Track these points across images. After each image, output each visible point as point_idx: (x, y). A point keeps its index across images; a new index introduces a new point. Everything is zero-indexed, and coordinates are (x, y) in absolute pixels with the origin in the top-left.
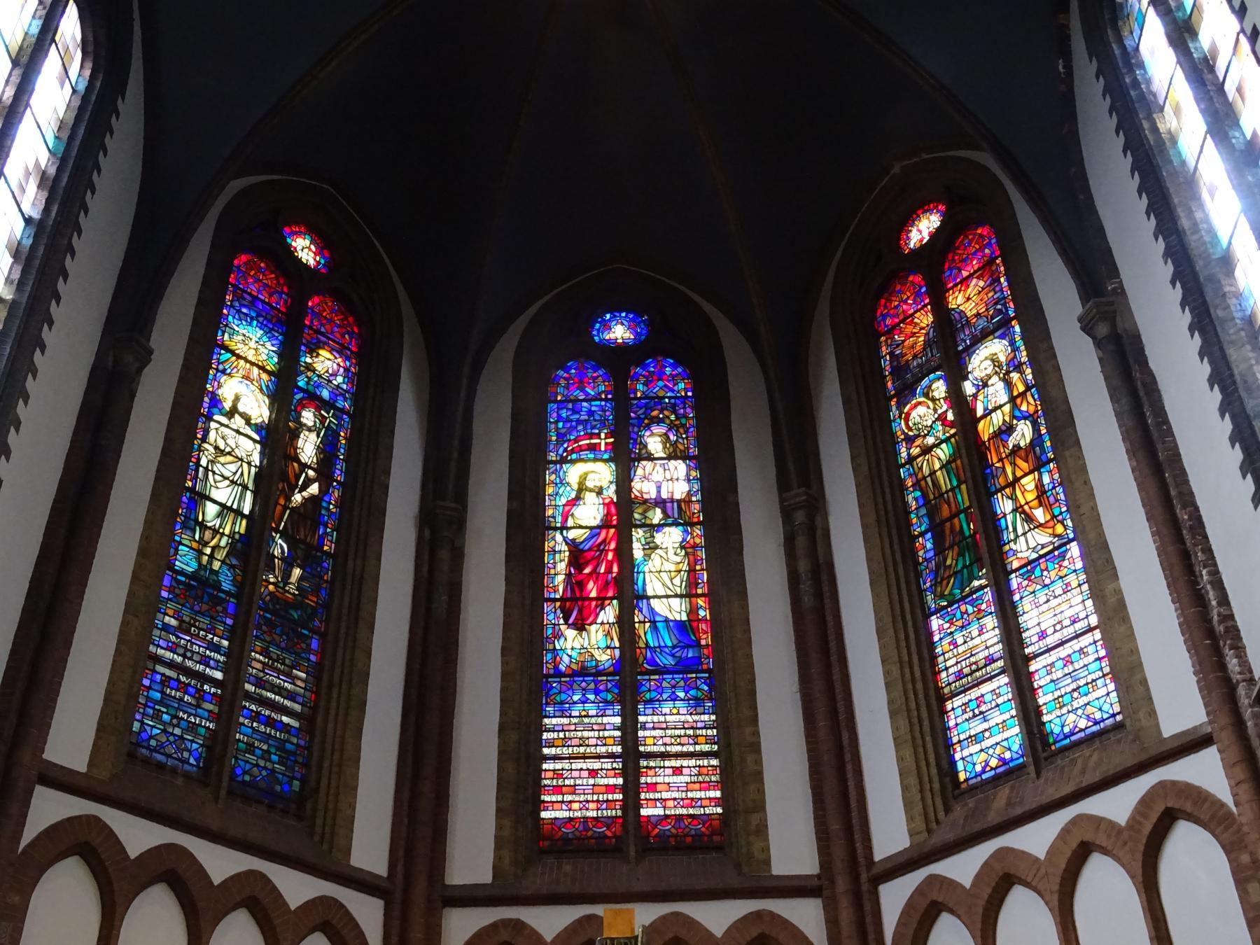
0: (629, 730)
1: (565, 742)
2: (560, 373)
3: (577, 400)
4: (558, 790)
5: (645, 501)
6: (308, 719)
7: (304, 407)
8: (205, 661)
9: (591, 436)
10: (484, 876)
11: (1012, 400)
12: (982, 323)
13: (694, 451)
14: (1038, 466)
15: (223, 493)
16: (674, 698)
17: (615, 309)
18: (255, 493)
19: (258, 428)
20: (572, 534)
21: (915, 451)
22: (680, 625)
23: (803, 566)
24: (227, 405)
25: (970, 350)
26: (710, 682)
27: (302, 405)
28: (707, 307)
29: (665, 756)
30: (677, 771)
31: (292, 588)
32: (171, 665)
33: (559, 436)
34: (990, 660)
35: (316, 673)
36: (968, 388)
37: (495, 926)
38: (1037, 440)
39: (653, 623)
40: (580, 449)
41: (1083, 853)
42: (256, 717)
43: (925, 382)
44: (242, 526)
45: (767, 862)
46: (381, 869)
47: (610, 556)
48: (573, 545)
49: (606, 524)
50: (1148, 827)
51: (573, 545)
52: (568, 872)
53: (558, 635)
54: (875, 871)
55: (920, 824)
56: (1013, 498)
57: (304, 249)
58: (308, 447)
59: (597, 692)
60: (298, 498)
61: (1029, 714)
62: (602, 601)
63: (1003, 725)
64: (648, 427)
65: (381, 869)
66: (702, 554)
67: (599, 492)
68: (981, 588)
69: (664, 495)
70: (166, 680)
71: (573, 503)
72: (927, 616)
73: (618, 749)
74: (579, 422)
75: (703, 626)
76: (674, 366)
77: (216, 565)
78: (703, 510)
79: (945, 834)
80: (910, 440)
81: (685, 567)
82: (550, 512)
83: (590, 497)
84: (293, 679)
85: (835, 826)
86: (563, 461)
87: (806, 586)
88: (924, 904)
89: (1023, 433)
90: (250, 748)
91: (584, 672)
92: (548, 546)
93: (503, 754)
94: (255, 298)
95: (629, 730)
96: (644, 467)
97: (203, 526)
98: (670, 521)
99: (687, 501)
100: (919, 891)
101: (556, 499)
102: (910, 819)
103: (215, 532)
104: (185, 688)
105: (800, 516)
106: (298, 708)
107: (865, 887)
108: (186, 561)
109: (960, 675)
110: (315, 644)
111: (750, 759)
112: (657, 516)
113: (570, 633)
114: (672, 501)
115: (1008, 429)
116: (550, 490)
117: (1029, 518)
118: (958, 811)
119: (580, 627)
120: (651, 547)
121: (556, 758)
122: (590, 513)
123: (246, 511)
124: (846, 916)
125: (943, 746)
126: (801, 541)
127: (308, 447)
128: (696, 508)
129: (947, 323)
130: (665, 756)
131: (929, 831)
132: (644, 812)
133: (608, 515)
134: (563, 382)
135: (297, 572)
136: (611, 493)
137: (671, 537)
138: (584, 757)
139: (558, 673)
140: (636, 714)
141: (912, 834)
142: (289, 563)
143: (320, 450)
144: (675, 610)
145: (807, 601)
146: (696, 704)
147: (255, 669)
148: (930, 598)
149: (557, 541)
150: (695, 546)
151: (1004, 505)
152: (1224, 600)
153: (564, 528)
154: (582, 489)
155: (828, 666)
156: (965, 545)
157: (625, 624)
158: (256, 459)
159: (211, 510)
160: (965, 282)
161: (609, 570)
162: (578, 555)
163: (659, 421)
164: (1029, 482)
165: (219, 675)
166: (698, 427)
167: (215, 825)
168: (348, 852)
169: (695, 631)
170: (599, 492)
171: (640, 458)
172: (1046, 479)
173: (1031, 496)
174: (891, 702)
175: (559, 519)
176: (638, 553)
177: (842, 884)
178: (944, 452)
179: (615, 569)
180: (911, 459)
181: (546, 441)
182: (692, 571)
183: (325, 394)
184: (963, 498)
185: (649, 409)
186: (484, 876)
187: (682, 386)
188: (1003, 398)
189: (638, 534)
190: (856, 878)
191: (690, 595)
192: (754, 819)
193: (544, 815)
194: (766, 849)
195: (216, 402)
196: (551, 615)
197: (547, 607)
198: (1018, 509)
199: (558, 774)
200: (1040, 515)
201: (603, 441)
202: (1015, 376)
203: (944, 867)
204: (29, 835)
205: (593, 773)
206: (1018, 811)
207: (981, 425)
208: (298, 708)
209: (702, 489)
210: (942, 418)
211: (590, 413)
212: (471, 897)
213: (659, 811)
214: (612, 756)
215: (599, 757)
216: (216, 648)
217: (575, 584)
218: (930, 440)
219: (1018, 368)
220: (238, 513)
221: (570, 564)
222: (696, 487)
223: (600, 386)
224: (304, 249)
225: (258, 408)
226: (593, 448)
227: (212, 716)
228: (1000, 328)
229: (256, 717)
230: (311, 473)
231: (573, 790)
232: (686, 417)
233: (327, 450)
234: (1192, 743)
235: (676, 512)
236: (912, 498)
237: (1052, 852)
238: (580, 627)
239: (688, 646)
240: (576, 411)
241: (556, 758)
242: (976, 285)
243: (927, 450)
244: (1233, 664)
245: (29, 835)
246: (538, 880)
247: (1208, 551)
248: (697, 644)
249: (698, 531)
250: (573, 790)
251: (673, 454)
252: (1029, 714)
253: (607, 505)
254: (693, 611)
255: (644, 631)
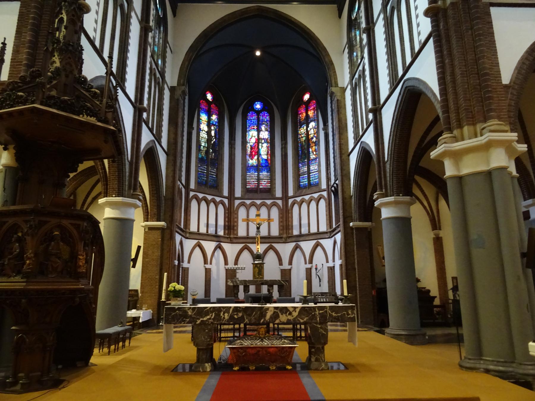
0: (258, 175)
1: (249, 177)
2: (249, 114)
3: (251, 120)
4: (249, 184)
5: (261, 139)
6: (217, 175)
7: (212, 126)
8: (204, 170)
9: (254, 126)
10: (240, 196)
11: (314, 133)
12: (312, 119)
13: (269, 130)
14: (315, 145)
15: (203, 144)
16: (265, 171)
17: (257, 101)
18: (207, 143)
19: (206, 132)
20: (251, 144)
21: (301, 137)
22: (266, 160)
23: (283, 153)
24: (202, 130)
25: (310, 123)
26: (270, 169)
27: (212, 126)
28: (272, 104)
29: (263, 179)
30: (265, 181)
31: (213, 157)
32: (200, 171)
33: (249, 126)
34: (306, 172)
35: (217, 169)
36: (309, 129)
37: (241, 202)
38: (316, 141)
39: (262, 160)
40: (252, 129)
41: (311, 200)
42: (210, 176)
43: (303, 126)
44: (206, 149)
45: (275, 195)
46: (227, 195)
47: (256, 148)
48: (251, 146)
49: (256, 142)
50: (318, 199)
51: (251, 146)
52: (251, 195)
53: (249, 161)
54: (289, 197)
55: (294, 193)
56: (312, 149)
57: (209, 97)
58: (213, 133)
59: (254, 169)
60: (212, 142)
61: (309, 180)
62: (255, 155)
63: (306, 181)
64: (262, 125)
65: (227, 195)
66: (269, 148)
67: (255, 137)
68: (306, 161)
69: (264, 138)
70: (200, 174)
71: (251, 138)
72: (299, 163)
73: (257, 178)
74: (252, 124)
75: (269, 160)
76: (267, 113)
77: (204, 156)
78: (270, 141)
79: (297, 195)
80: (300, 135)
81: (267, 150)
82: (247, 140)
83: (253, 137)
84: (214, 170)
85: (284, 191)
86: (249, 131)
87: (283, 157)
88: (293, 203)
89: (314, 139)
90: (210, 181)
91: (252, 166)
92: (247, 146)
93: (242, 179)
94: (203, 109)
95: (258, 175)
96: (261, 133)
97: (201, 150)
98: (265, 142)
99: (267, 139)
100: (293, 201)
101: (248, 138)
102: (293, 192)
103: (203, 150)
104: (202, 174)
105: (283, 146)
106: (215, 174)
107: (287, 199)
108: (200, 157)
109: (302, 173)
110: (216, 165)
111: (274, 181)
112: (263, 141)
113: (250, 160)
114: (265, 139)
115: (312, 138)
116: (247, 136)
117: (313, 153)
118: (299, 191)
119: (252, 159)
120: (262, 147)
121: (248, 179)
122: (253, 140)
123: (206, 146)
124: (284, 203)
125: (299, 182)
126: (283, 149)
127: (213, 133)
128: (269, 140)
129: (307, 116)
130: (263, 179)
131: (295, 194)
132: (260, 187)
133: (256, 141)
134: (249, 116)
135: (213, 154)
136: (256, 137)
137: (265, 145)
138: (252, 179)
139: (249, 167)
140: (259, 173)
141: (293, 194)
142: (212, 153)
143: (215, 133)
144: (265, 157)
145: (284, 159)
146: (267, 172)
147: (210, 170)
148: (300, 160)
149: (248, 145)
150: (268, 147)
151: (311, 150)
152: (330, 175)
153: (249, 143)
154: (252, 136)
155: (285, 169)
156: (305, 154)
157: (258, 159)
158: (207, 138)
159: (202, 147)
160: (311, 110)
161: (256, 150)
162: (252, 148)
163: (264, 124)
164: (314, 147)
165: (206, 172)
166: (270, 125)
167: (209, 193)
168: (223, 194)
169: (268, 161)
170: (255, 137)
171: (261, 131)
172: (316, 148)
173: (314, 150)
174: (293, 176)
175: (249, 141)
176: (260, 147)
177: (284, 199)
178: (304, 138)
179: (257, 150)
180: (300, 138)
181: (247, 127)
182: (268, 151)
183: (214, 123)
184: (306, 147)
185: (262, 121)
186: (240, 196)
187: (268, 117)
188: (313, 133)
189: (260, 144)
190: (286, 198)
191: (267, 155)
192: (274, 189)
193: (247, 187)
194: (275, 194)
195: (200, 129)
196: (248, 158)
197: (247, 156)
198: (312, 151)
199: (249, 181)
200: (315, 153)
201: (255, 127)
202: (315, 130)
203: (296, 199)
204: (190, 197)
205: (253, 181)
206: (305, 194)
207: (310, 136)
208: (215, 174)
209: (270, 137)
210: (305, 132)
211: (254, 122)
212: (238, 199)
213: (262, 187)
214: (256, 179)
215: (254, 179)
216: (205, 168)
217: (251, 152)
218: (303, 136)
219: (316, 128)
220: (205, 147)
221: (251, 149)
222: (269, 136)
223: (255, 117)
224: (209, 97)
225: (206, 129)
226: (254, 129)
227: (206, 178)
228: (314, 121)
229: (210, 176)
230: (214, 137)
231: (251, 184)
232: (268, 123)
233: (215, 133)
234: (324, 190)
235: (266, 141)
236: (299, 144)
237: (308, 199)
238: (252, 159)
239: (267, 163)
240: (251, 122)
241: (248, 179)
242: (312, 111)
243: (302, 137)
244: (330, 183)
245: (190, 197)
246: (247, 197)
247: (330, 168)
248: (268, 163)
249: (269, 144)
250: (251, 184)
251: (266, 130)
252: (309, 180)
253: (256, 139)
254: (268, 157)
255: (261, 160)
